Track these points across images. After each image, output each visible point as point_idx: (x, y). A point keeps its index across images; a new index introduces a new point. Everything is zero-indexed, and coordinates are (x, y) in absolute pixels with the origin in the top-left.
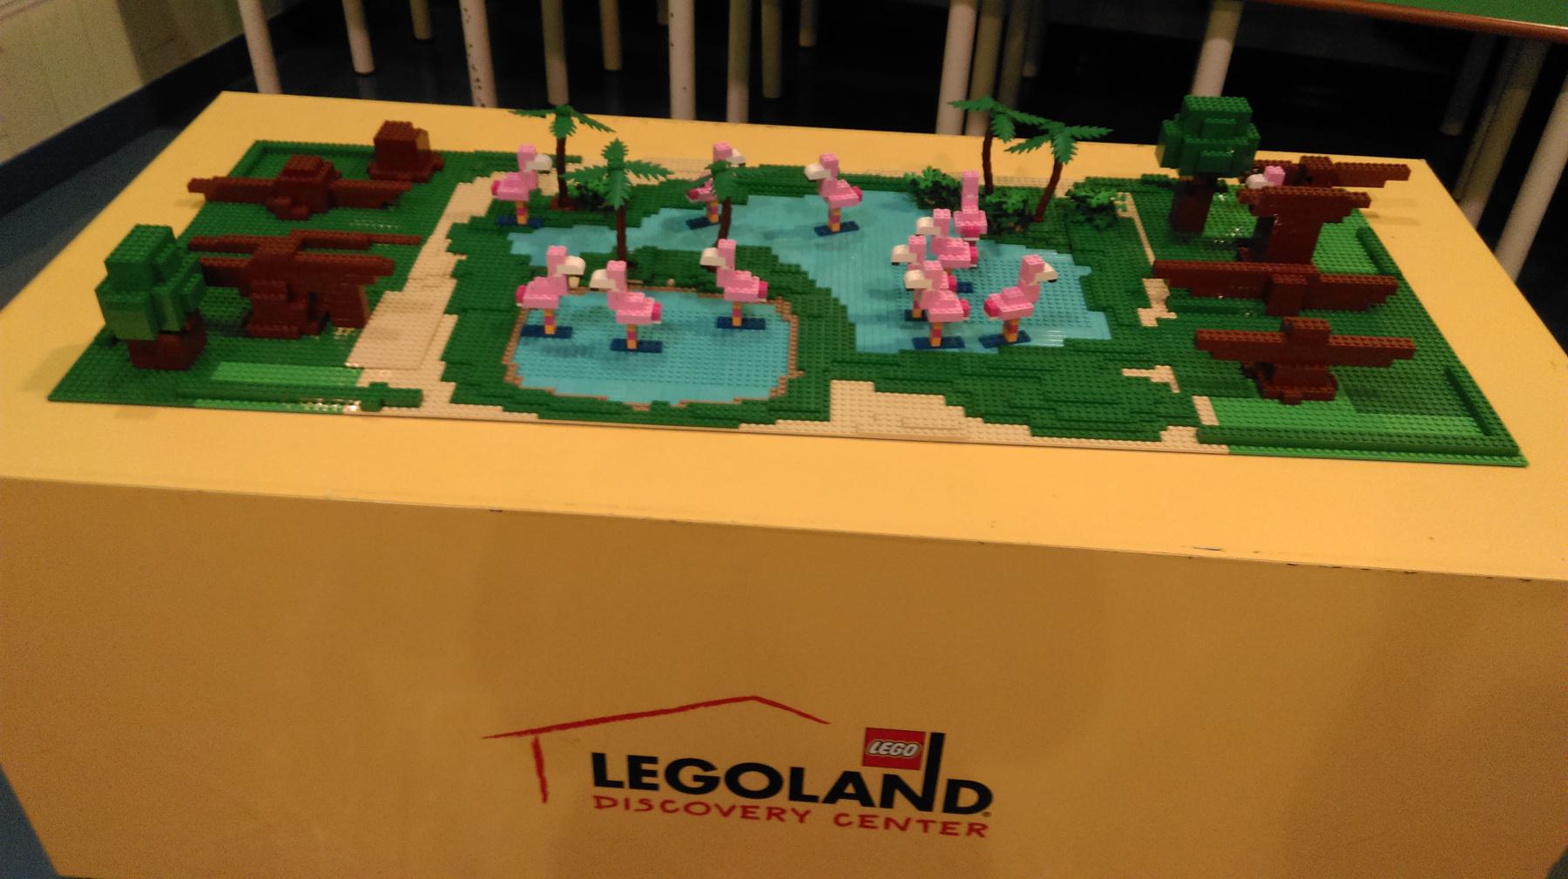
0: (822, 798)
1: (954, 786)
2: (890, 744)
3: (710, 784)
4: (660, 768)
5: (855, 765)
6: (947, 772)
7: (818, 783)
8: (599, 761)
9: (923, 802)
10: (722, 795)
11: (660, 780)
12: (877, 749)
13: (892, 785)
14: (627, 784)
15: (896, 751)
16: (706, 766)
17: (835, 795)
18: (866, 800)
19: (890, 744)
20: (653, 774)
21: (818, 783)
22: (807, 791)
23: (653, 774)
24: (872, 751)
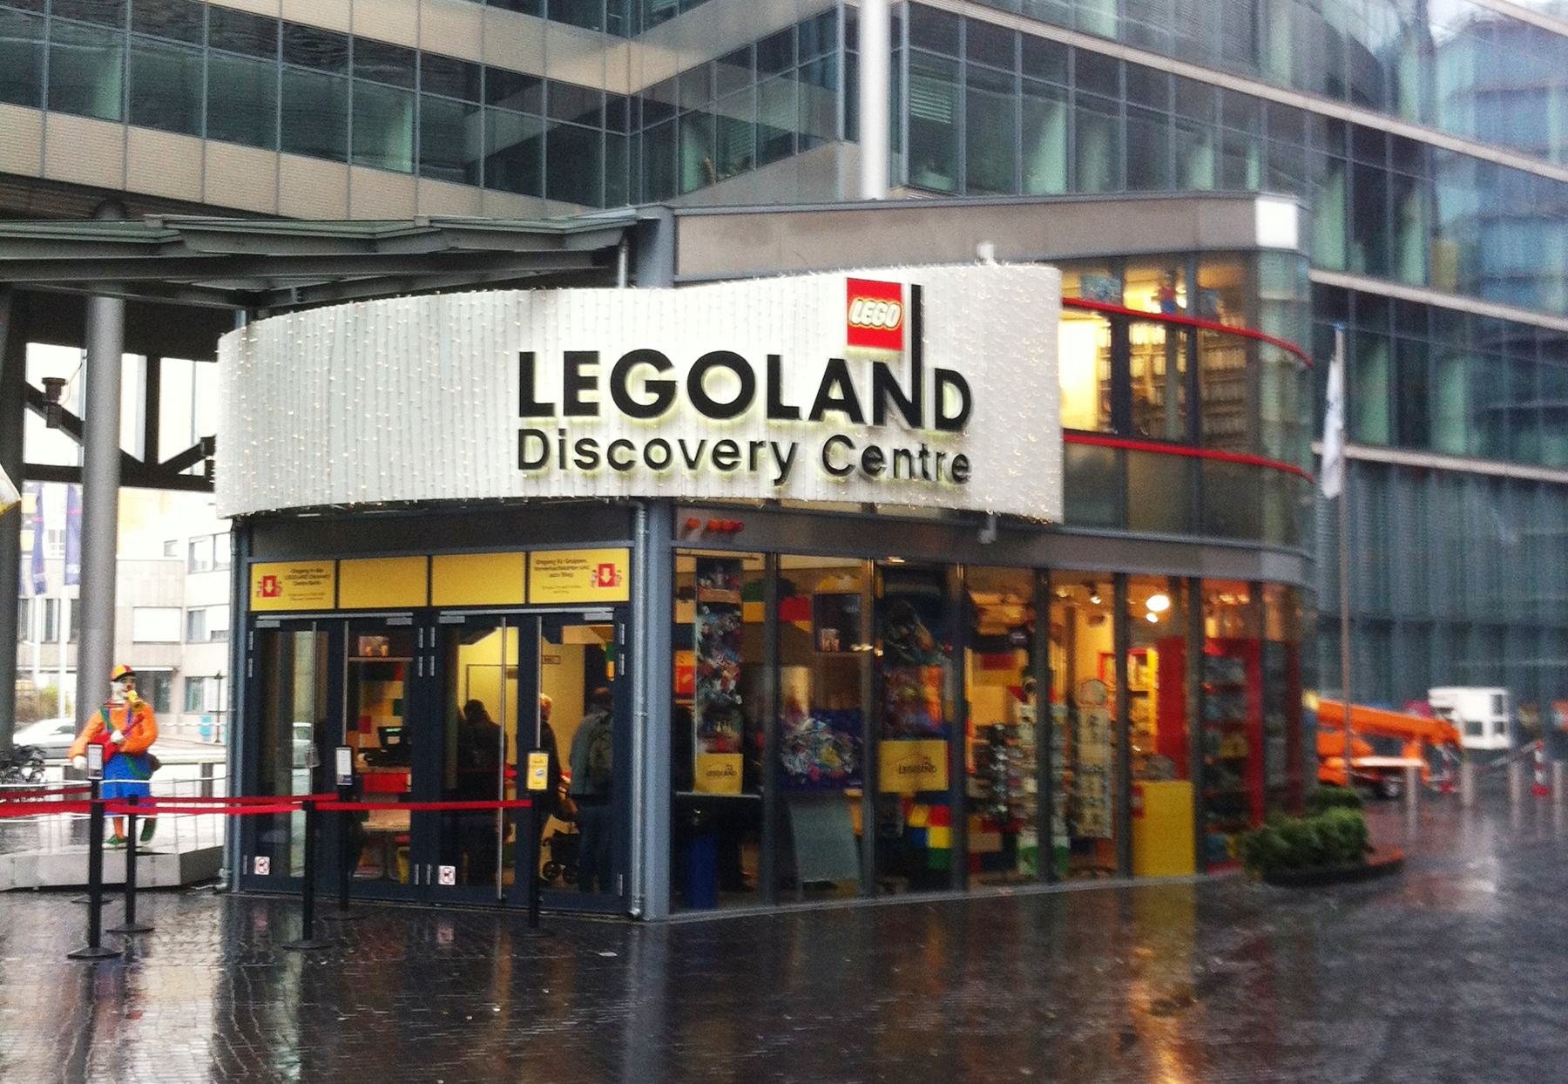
3: (665, 391)
4: (602, 372)
6: (932, 362)
7: (800, 390)
8: (527, 361)
9: (913, 414)
10: (684, 414)
11: (602, 395)
14: (559, 408)
16: (661, 362)
17: (823, 403)
18: (856, 416)
20: (591, 383)
21: (800, 390)
22: (787, 401)
23: (591, 383)
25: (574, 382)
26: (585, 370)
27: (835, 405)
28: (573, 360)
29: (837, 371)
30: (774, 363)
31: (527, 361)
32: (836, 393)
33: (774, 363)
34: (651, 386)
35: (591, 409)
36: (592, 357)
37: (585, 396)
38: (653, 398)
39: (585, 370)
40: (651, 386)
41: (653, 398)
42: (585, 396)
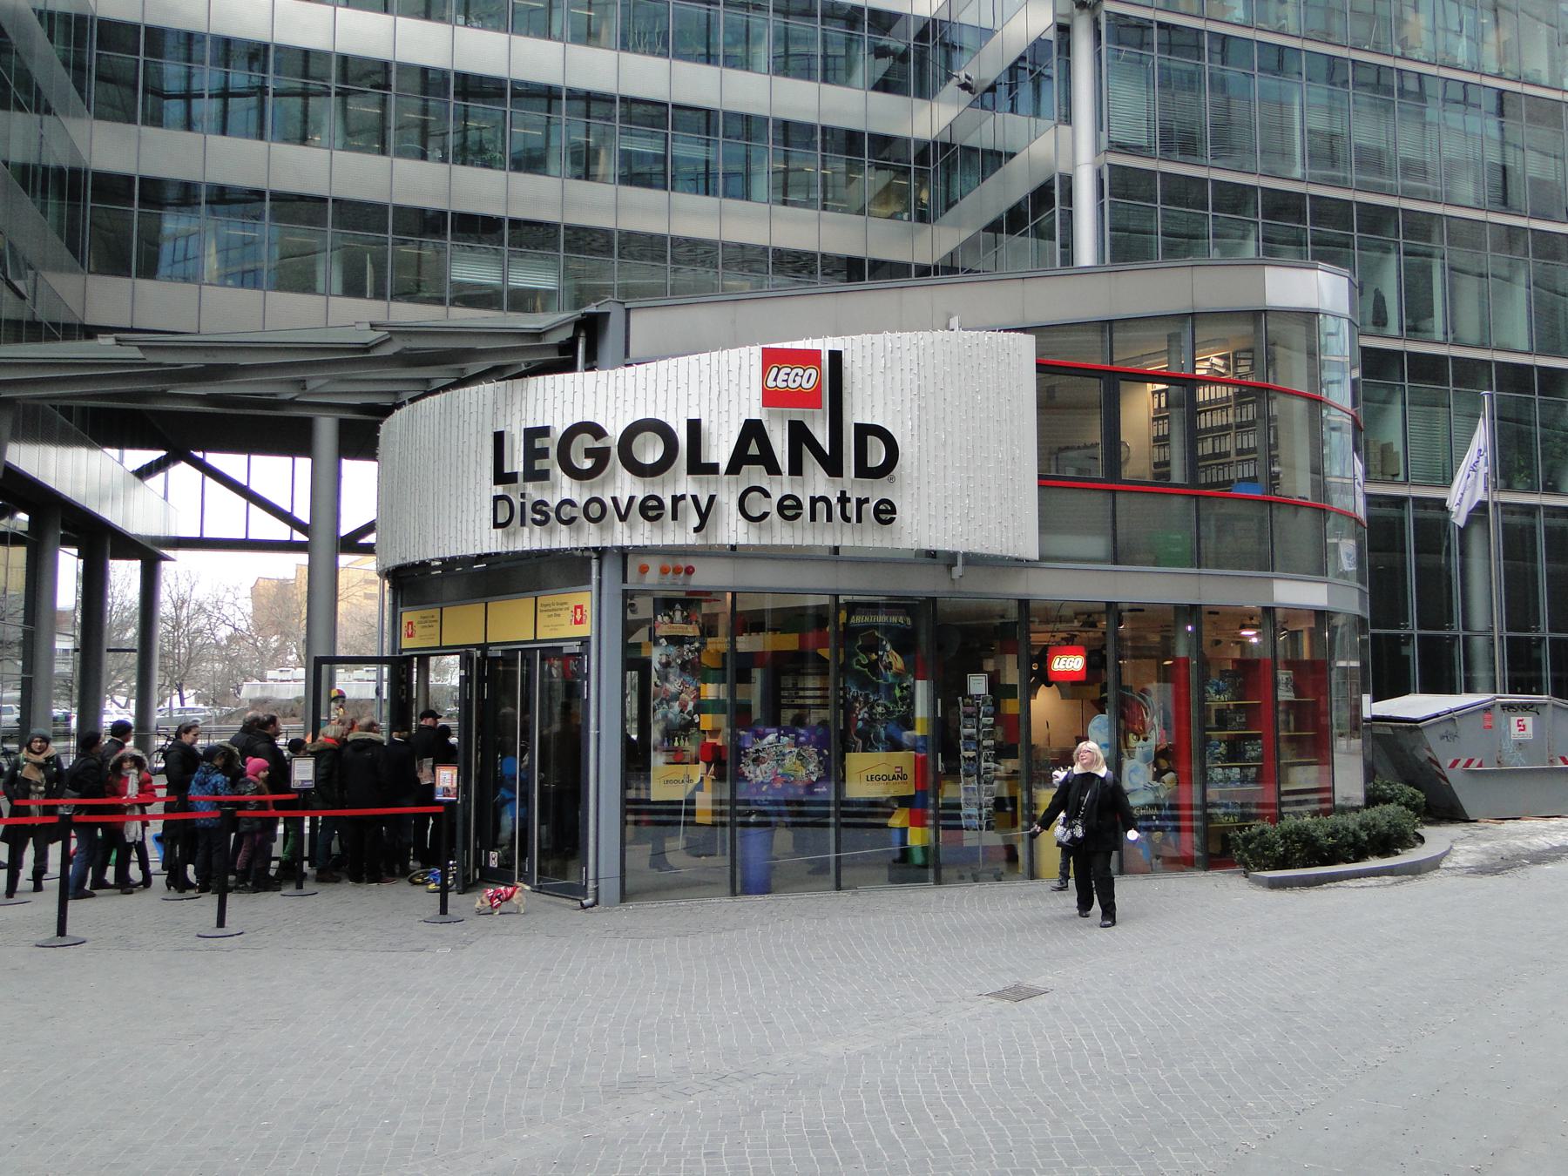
0: (723, 467)
1: (863, 431)
2: (788, 370)
3: (600, 458)
5: (756, 412)
6: (857, 412)
8: (499, 438)
9: (833, 466)
12: (775, 380)
13: (799, 435)
15: (794, 381)
16: (597, 431)
17: (739, 460)
18: (773, 469)
19: (788, 370)
20: (544, 453)
21: (720, 450)
23: (544, 453)
24: (771, 383)
25: (533, 453)
26: (539, 443)
27: (753, 460)
28: (532, 434)
29: (753, 430)
30: (694, 427)
31: (499, 438)
32: (754, 449)
33: (694, 427)
34: (589, 453)
35: (544, 475)
36: (544, 431)
37: (539, 465)
38: (587, 464)
39: (538, 444)
40: (589, 453)
41: (587, 464)
42: (539, 465)
